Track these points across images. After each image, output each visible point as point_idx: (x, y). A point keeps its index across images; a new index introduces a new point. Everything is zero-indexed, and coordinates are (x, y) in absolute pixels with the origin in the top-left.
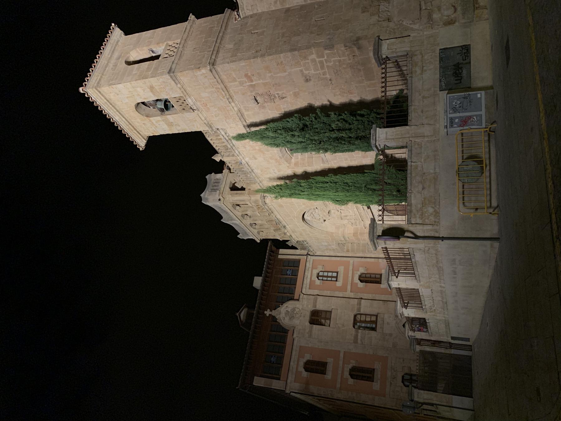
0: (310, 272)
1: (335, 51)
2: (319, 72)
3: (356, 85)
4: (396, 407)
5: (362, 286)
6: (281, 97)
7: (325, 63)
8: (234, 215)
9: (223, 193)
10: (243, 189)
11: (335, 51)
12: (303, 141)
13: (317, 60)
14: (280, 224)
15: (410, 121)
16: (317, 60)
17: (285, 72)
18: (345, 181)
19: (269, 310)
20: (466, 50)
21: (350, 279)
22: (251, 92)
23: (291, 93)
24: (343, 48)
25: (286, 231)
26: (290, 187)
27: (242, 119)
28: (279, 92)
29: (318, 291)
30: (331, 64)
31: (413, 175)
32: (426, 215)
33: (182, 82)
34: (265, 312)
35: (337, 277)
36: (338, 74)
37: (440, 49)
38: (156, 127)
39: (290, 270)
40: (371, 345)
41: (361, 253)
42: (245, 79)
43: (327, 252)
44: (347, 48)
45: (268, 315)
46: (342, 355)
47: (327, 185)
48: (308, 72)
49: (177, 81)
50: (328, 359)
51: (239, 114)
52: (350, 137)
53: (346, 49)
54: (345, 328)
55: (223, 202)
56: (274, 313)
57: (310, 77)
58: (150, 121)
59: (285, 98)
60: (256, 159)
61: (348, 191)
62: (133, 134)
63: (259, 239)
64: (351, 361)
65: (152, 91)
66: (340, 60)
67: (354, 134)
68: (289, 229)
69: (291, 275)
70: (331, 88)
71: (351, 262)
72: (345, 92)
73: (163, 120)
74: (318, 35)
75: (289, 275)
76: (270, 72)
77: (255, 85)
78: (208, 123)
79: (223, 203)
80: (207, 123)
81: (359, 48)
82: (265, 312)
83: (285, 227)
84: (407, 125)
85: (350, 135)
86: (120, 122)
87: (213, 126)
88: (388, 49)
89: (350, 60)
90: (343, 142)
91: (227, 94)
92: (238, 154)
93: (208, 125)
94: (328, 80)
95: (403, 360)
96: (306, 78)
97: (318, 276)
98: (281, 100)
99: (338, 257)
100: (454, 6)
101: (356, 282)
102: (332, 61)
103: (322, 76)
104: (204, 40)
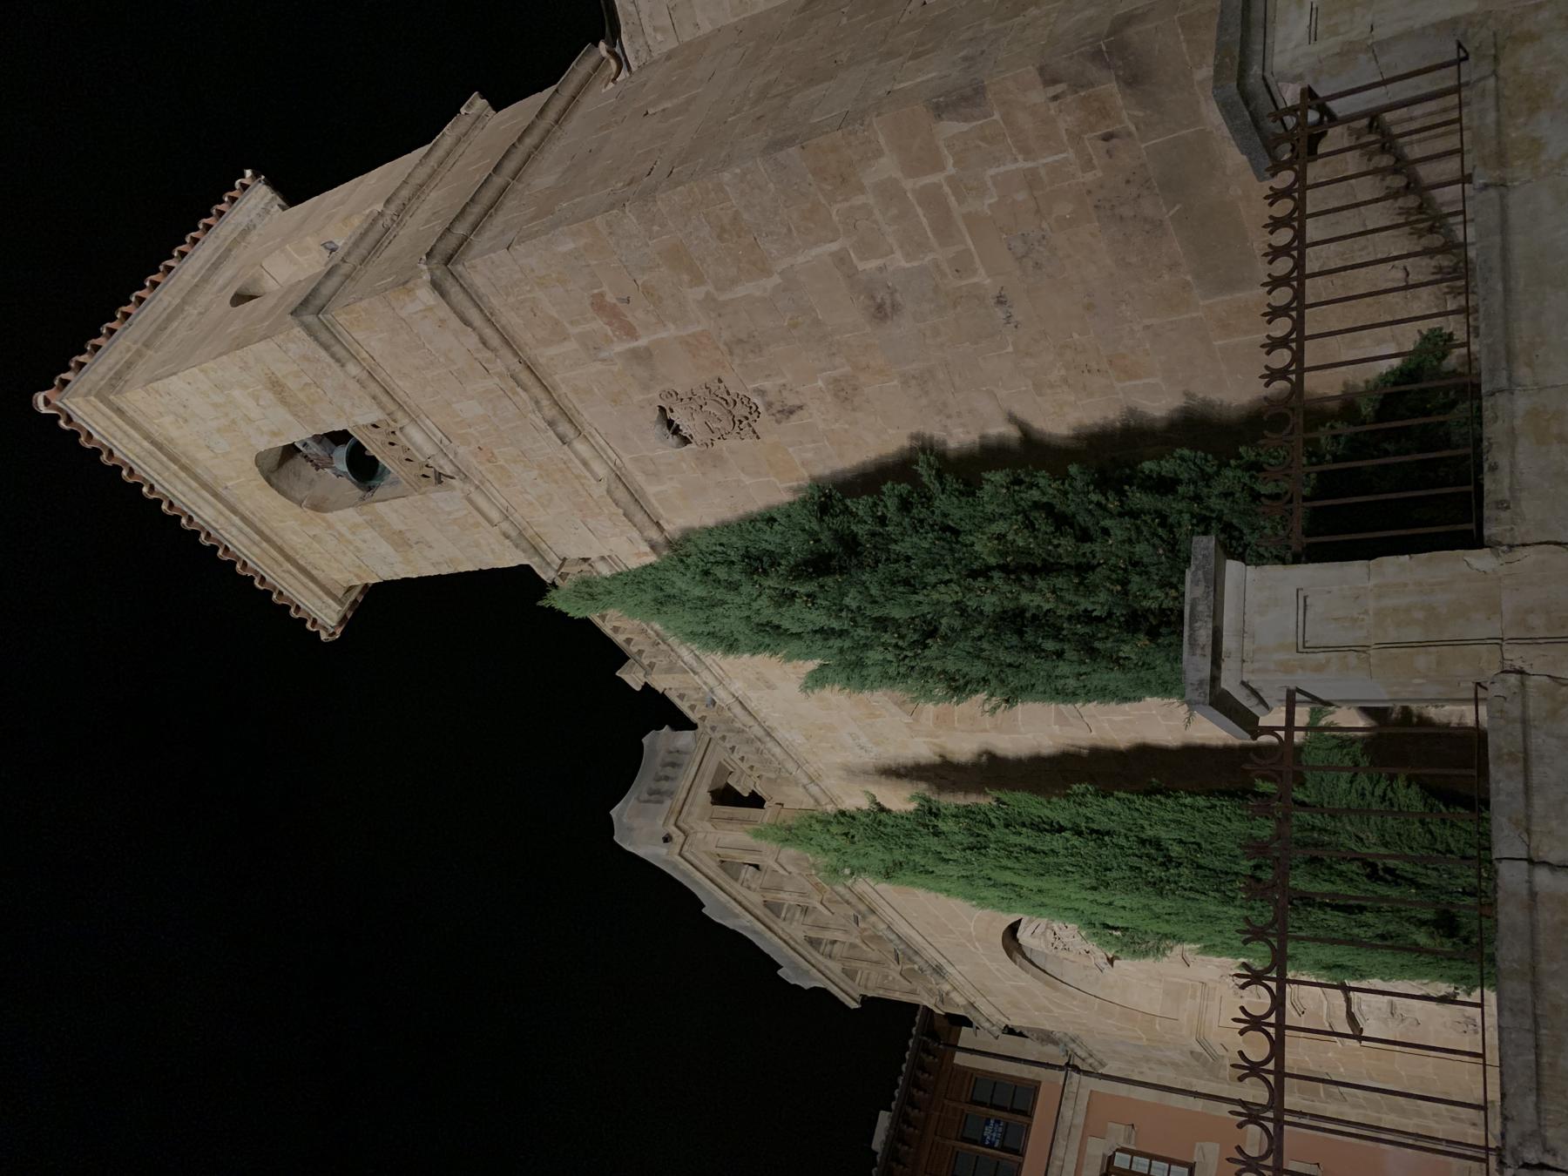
0: (1075, 1146)
1: (997, 116)
2: (930, 257)
3: (1147, 322)
6: (777, 406)
7: (952, 200)
8: (735, 900)
9: (680, 812)
10: (756, 801)
11: (997, 116)
12: (836, 625)
13: (908, 184)
14: (917, 959)
15: (1502, 505)
16: (908, 184)
17: (767, 272)
18: (1149, 833)
23: (820, 383)
24: (1038, 96)
25: (947, 987)
26: (889, 830)
27: (639, 517)
28: (767, 385)
33: (365, 355)
36: (1037, 265)
38: (358, 550)
39: (997, 1122)
41: (1297, 1095)
42: (599, 324)
44: (1060, 88)
47: (1055, 842)
48: (873, 264)
49: (337, 348)
51: (621, 493)
52: (1087, 618)
53: (1055, 98)
55: (678, 851)
57: (893, 292)
58: (330, 526)
59: (800, 412)
60: (770, 687)
61: (1158, 887)
62: (283, 579)
63: (856, 996)
65: (284, 402)
67: (1103, 596)
68: (960, 978)
69: (996, 1145)
70: (1010, 349)
72: (1094, 366)
73: (370, 523)
75: (991, 1146)
76: (698, 279)
77: (647, 349)
78: (520, 534)
79: (680, 854)
80: (514, 534)
81: (1134, 80)
83: (938, 970)
84: (1474, 541)
85: (1085, 604)
86: (222, 532)
87: (544, 546)
88: (1313, 36)
89: (1088, 165)
90: (1050, 645)
91: (545, 403)
92: (695, 664)
93: (524, 544)
94: (993, 301)
96: (873, 298)
98: (783, 424)
99: (1197, 1095)
102: (990, 183)
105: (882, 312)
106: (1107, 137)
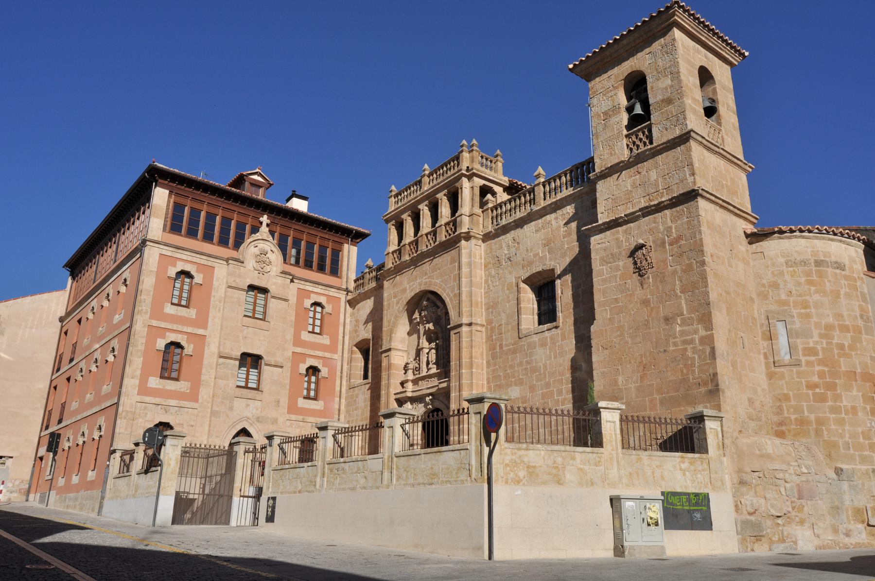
1: (709, 361)
4: (122, 412)
5: (300, 370)
11: (709, 361)
19: (269, 222)
20: (706, 524)
21: (312, 353)
22: (654, 242)
23: (649, 297)
29: (295, 302)
30: (690, 354)
31: (564, 454)
32: (516, 468)
34: (265, 217)
35: (313, 332)
37: (708, 494)
40: (215, 378)
43: (351, 321)
44: (712, 376)
45: (261, 219)
46: (201, 332)
56: (264, 229)
57: (672, 324)
64: (192, 346)
66: (694, 366)
71: (335, 356)
74: (728, 339)
77: (664, 247)
82: (265, 217)
94: (665, 349)
95: (192, 426)
97: (316, 304)
100: (755, 513)
101: (307, 362)
103: (671, 341)
104: (724, 182)
105: (667, 320)
106: (699, 384)
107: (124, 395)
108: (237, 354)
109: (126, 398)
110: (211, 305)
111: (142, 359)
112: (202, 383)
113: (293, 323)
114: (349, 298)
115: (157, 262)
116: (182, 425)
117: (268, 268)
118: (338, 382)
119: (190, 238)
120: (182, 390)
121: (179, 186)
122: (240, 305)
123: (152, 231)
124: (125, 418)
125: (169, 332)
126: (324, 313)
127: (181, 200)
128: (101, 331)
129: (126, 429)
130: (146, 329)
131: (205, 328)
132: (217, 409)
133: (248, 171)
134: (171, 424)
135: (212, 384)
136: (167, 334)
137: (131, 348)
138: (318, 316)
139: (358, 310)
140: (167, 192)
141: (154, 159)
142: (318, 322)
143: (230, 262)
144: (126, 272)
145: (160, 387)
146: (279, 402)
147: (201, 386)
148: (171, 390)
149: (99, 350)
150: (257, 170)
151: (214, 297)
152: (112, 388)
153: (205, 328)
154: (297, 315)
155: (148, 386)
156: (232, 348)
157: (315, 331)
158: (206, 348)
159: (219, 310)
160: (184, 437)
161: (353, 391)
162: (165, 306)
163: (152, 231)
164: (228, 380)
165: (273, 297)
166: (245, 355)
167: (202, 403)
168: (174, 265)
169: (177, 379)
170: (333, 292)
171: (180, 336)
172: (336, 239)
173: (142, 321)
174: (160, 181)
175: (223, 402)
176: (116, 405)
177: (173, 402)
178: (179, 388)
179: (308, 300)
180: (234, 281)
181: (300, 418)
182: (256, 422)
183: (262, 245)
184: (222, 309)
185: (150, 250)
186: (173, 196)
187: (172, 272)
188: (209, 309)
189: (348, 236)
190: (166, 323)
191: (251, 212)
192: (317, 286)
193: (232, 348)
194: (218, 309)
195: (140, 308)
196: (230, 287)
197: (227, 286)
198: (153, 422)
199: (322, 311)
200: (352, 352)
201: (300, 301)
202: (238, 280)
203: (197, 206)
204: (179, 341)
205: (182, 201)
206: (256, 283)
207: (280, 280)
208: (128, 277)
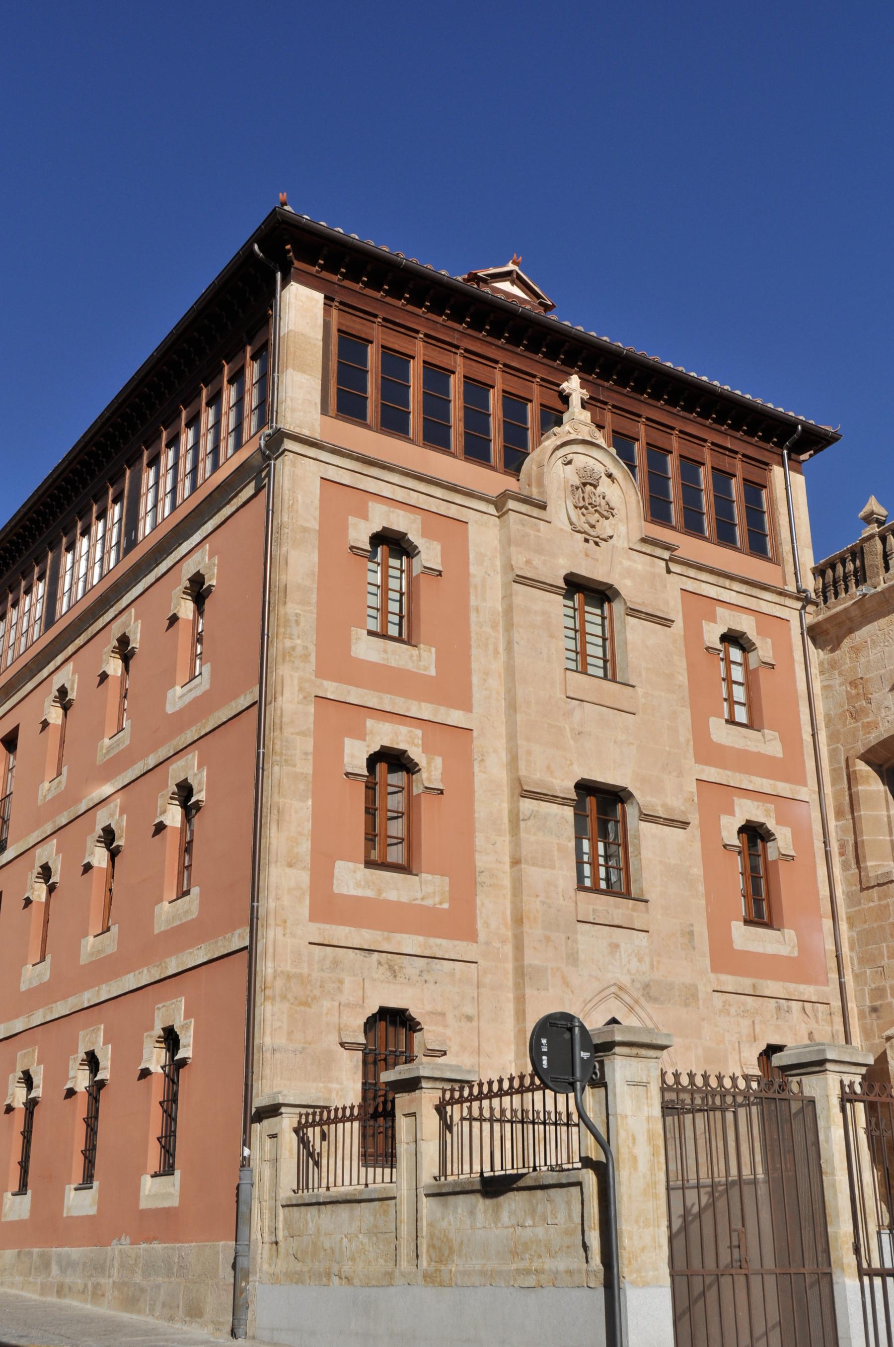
4: (275, 977)
5: (724, 834)
46: (456, 717)
50: (433, 650)
54: (572, 742)
64: (438, 761)
95: (469, 1018)
97: (732, 638)
101: (737, 810)
107: (271, 921)
108: (566, 786)
109: (280, 930)
110: (473, 635)
111: (310, 802)
112: (479, 879)
113: (686, 693)
114: (809, 620)
115: (317, 502)
116: (443, 1014)
117: (606, 527)
118: (822, 871)
119: (390, 435)
120: (429, 902)
121: (347, 283)
122: (552, 636)
123: (293, 410)
124: (284, 997)
125: (371, 718)
126: (753, 665)
127: (357, 326)
128: (110, 748)
129: (290, 1033)
130: (311, 709)
131: (466, 706)
132: (537, 962)
133: (487, 268)
134: (415, 1012)
135: (507, 882)
136: (370, 723)
137: (276, 769)
138: (738, 674)
139: (856, 650)
140: (319, 297)
141: (283, 196)
142: (739, 693)
143: (511, 504)
144: (196, 556)
145: (369, 893)
146: (691, 933)
147: (479, 889)
148: (399, 904)
149: (118, 801)
150: (511, 267)
151: (477, 610)
152: (202, 904)
153: (466, 706)
154: (691, 669)
155: (336, 891)
156: (548, 767)
157: (737, 720)
158: (476, 769)
159: (496, 652)
160: (663, 1048)
161: (886, 896)
162: (353, 637)
163: (293, 410)
164: (552, 867)
165: (633, 612)
166: (585, 788)
167: (487, 943)
168: (364, 515)
169: (405, 869)
170: (767, 604)
171: (404, 730)
172: (751, 452)
173: (296, 682)
174: (297, 264)
175: (548, 939)
176: (245, 952)
177: (410, 943)
178: (419, 895)
179: (712, 625)
180: (528, 562)
181: (745, 983)
182: (642, 1001)
183: (583, 459)
184: (501, 648)
185: (294, 464)
186: (335, 313)
187: (361, 535)
188: (469, 647)
189: (780, 445)
190: (361, 691)
191: (537, 365)
192: (727, 583)
193: (548, 767)
194: (491, 647)
195: (288, 643)
196: (522, 580)
197: (511, 576)
198: (362, 1007)
199: (746, 659)
200: (851, 778)
201: (693, 632)
202: (537, 561)
203: (399, 343)
204: (402, 746)
205: (357, 326)
206: (583, 570)
207: (640, 563)
208: (210, 567)
